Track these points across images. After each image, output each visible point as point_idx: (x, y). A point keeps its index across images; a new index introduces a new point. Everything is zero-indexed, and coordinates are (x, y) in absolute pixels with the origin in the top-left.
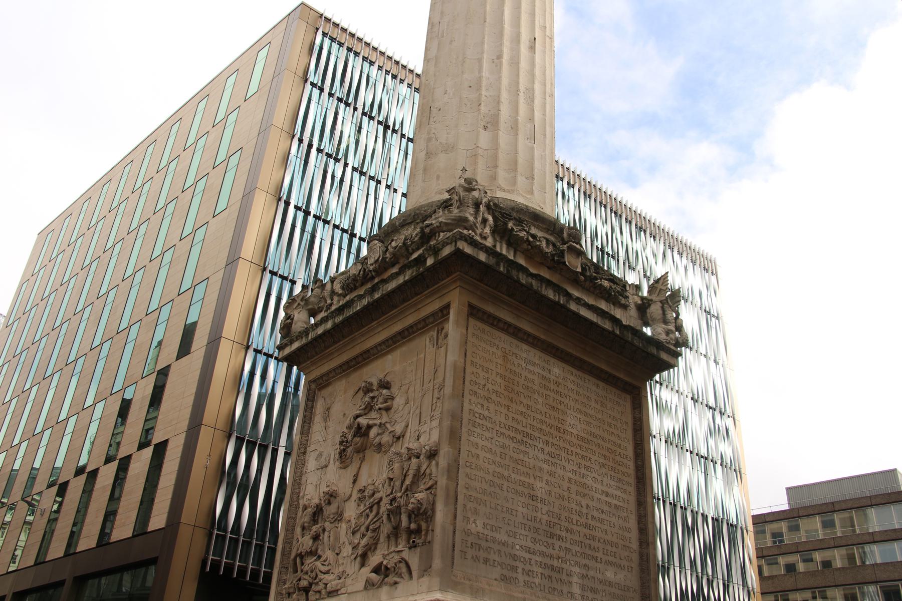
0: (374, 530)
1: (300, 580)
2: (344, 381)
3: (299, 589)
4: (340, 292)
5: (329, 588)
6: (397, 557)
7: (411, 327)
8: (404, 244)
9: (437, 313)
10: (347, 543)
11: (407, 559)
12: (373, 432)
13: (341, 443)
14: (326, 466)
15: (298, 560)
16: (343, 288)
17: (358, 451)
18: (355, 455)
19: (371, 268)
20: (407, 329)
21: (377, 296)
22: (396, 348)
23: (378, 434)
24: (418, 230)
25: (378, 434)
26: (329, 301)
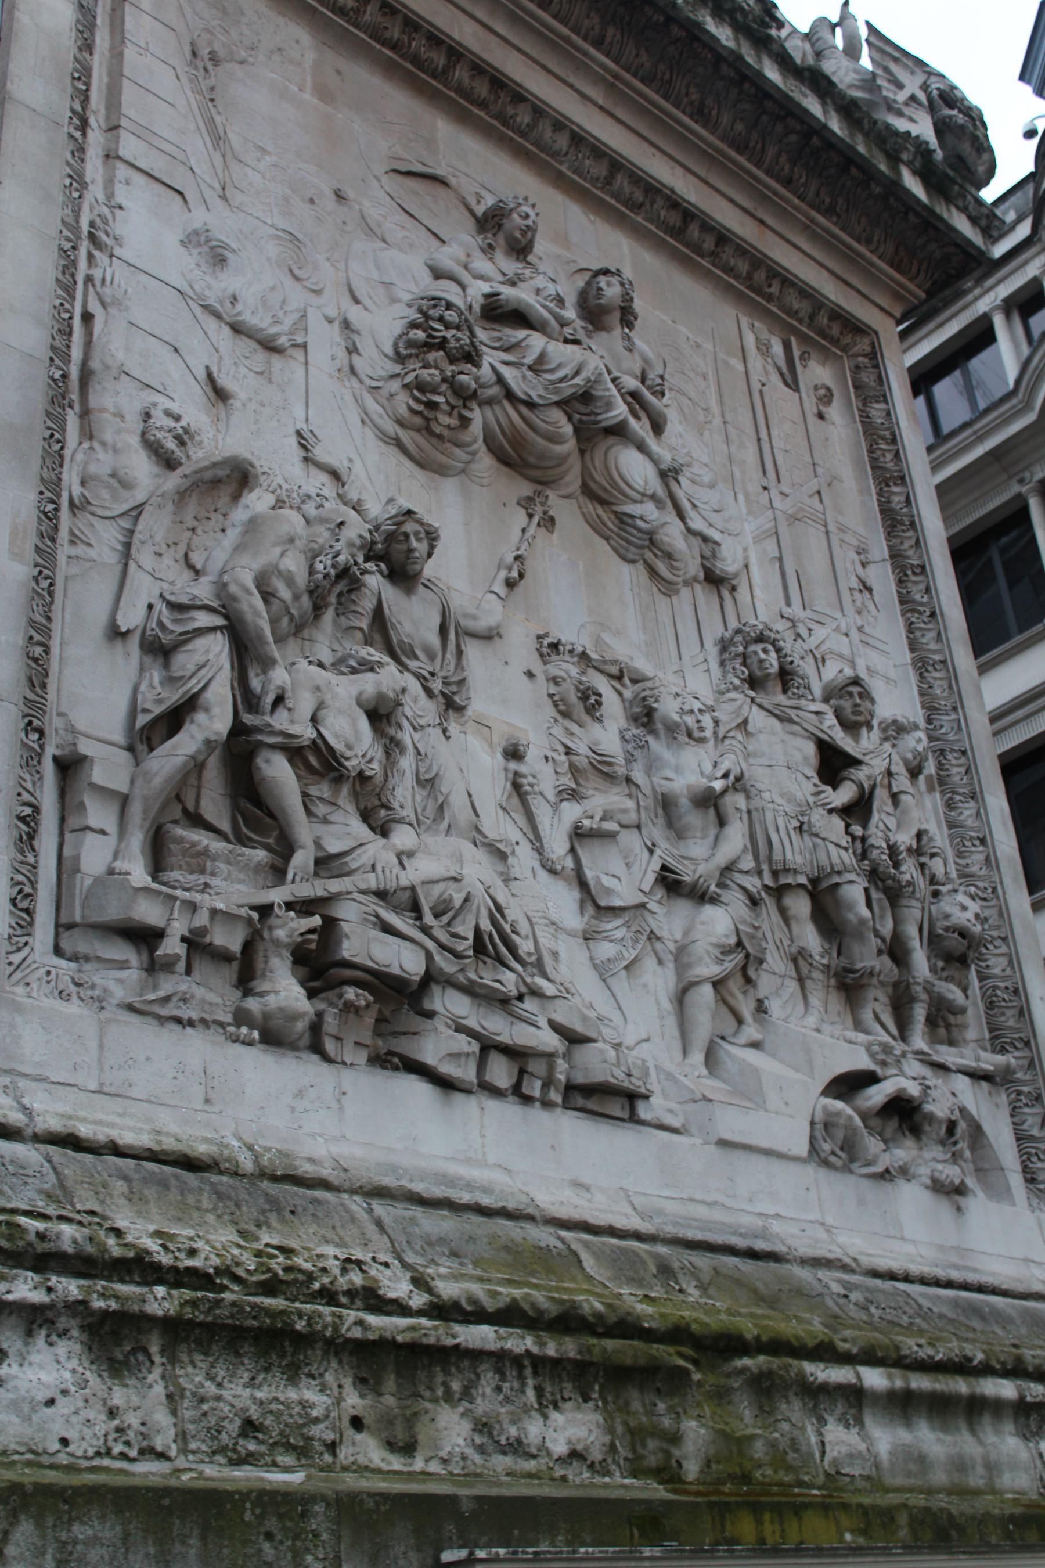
5: (596, 1064)
7: (723, 238)
12: (633, 467)
14: (270, 346)
17: (514, 456)
18: (485, 462)
20: (707, 226)
22: (619, 220)
23: (653, 497)
25: (653, 497)
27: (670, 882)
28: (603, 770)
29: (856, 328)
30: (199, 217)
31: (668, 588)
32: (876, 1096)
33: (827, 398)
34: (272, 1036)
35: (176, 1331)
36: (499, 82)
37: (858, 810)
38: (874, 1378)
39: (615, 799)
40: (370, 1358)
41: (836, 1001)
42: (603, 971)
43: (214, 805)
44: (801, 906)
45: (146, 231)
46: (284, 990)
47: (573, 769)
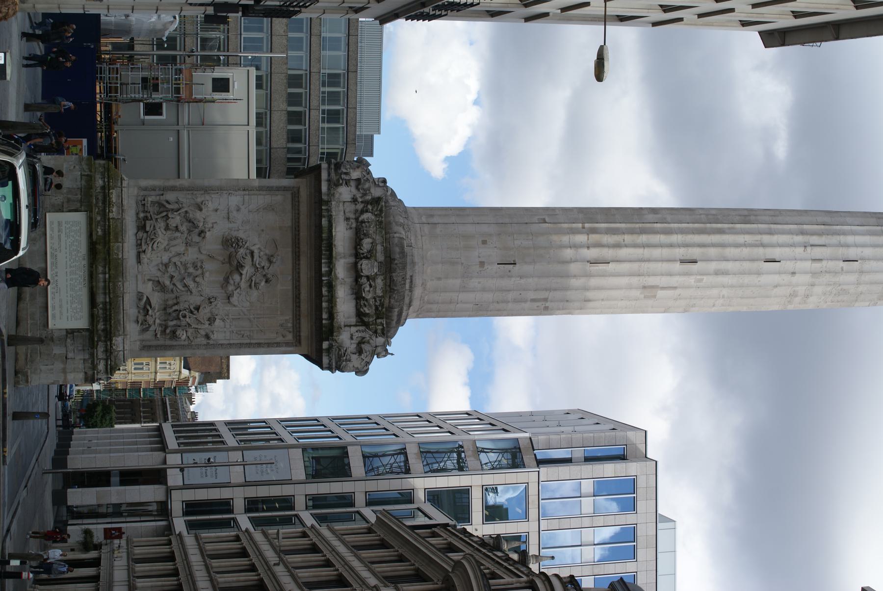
0: (172, 291)
1: (152, 219)
2: (290, 224)
3: (146, 218)
4: (360, 219)
5: (142, 256)
6: (151, 322)
7: (299, 307)
8: (364, 298)
9: (299, 332)
10: (171, 255)
11: (151, 329)
12: (236, 277)
13: (238, 240)
15: (165, 214)
16: (363, 222)
17: (230, 257)
19: (359, 265)
21: (324, 291)
24: (367, 312)
26: (360, 200)
27: (172, 277)
28: (186, 269)
29: (300, 343)
30: (242, 207)
31: (222, 287)
32: (148, 307)
33: (284, 337)
34: (137, 214)
35: (104, 193)
36: (299, 256)
37: (192, 312)
38: (107, 276)
39: (183, 272)
40: (104, 210)
41: (163, 307)
42: (158, 265)
43: (162, 209)
44: (175, 301)
45: (235, 200)
46: (142, 215)
47: (185, 265)
